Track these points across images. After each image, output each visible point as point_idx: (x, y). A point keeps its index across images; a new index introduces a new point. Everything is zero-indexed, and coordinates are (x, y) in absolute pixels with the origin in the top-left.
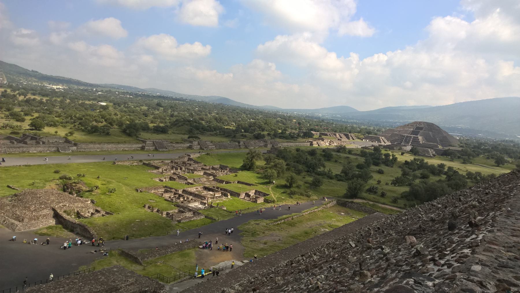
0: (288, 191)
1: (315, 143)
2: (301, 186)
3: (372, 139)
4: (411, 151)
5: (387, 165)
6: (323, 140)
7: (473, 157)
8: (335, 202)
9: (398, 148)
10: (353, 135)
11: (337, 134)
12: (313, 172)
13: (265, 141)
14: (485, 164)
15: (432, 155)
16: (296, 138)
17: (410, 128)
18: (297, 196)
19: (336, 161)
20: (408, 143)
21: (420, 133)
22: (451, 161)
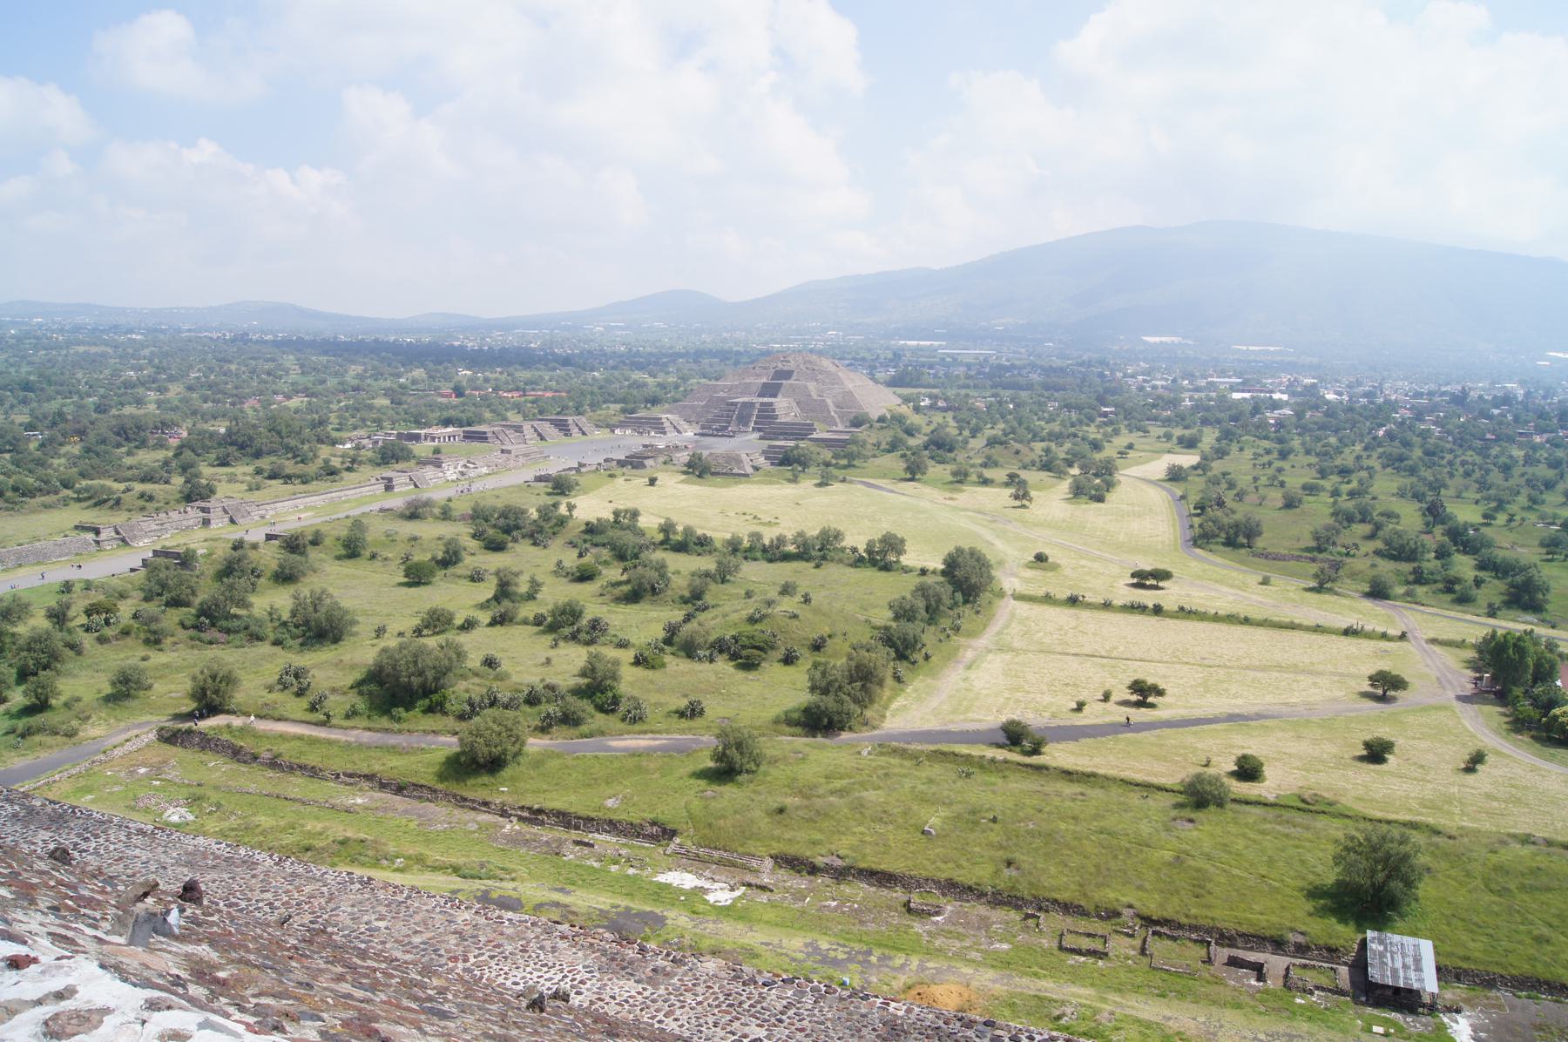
0: (21, 724)
1: (400, 480)
2: (78, 700)
3: (640, 426)
4: (689, 465)
5: (535, 544)
6: (438, 464)
7: (866, 458)
8: (152, 736)
9: (661, 459)
10: (582, 420)
11: (527, 427)
12: (213, 625)
13: (203, 510)
14: (884, 476)
15: (749, 470)
16: (348, 469)
17: (758, 376)
18: (37, 738)
19: (373, 557)
20: (746, 424)
21: (783, 390)
22: (789, 481)
